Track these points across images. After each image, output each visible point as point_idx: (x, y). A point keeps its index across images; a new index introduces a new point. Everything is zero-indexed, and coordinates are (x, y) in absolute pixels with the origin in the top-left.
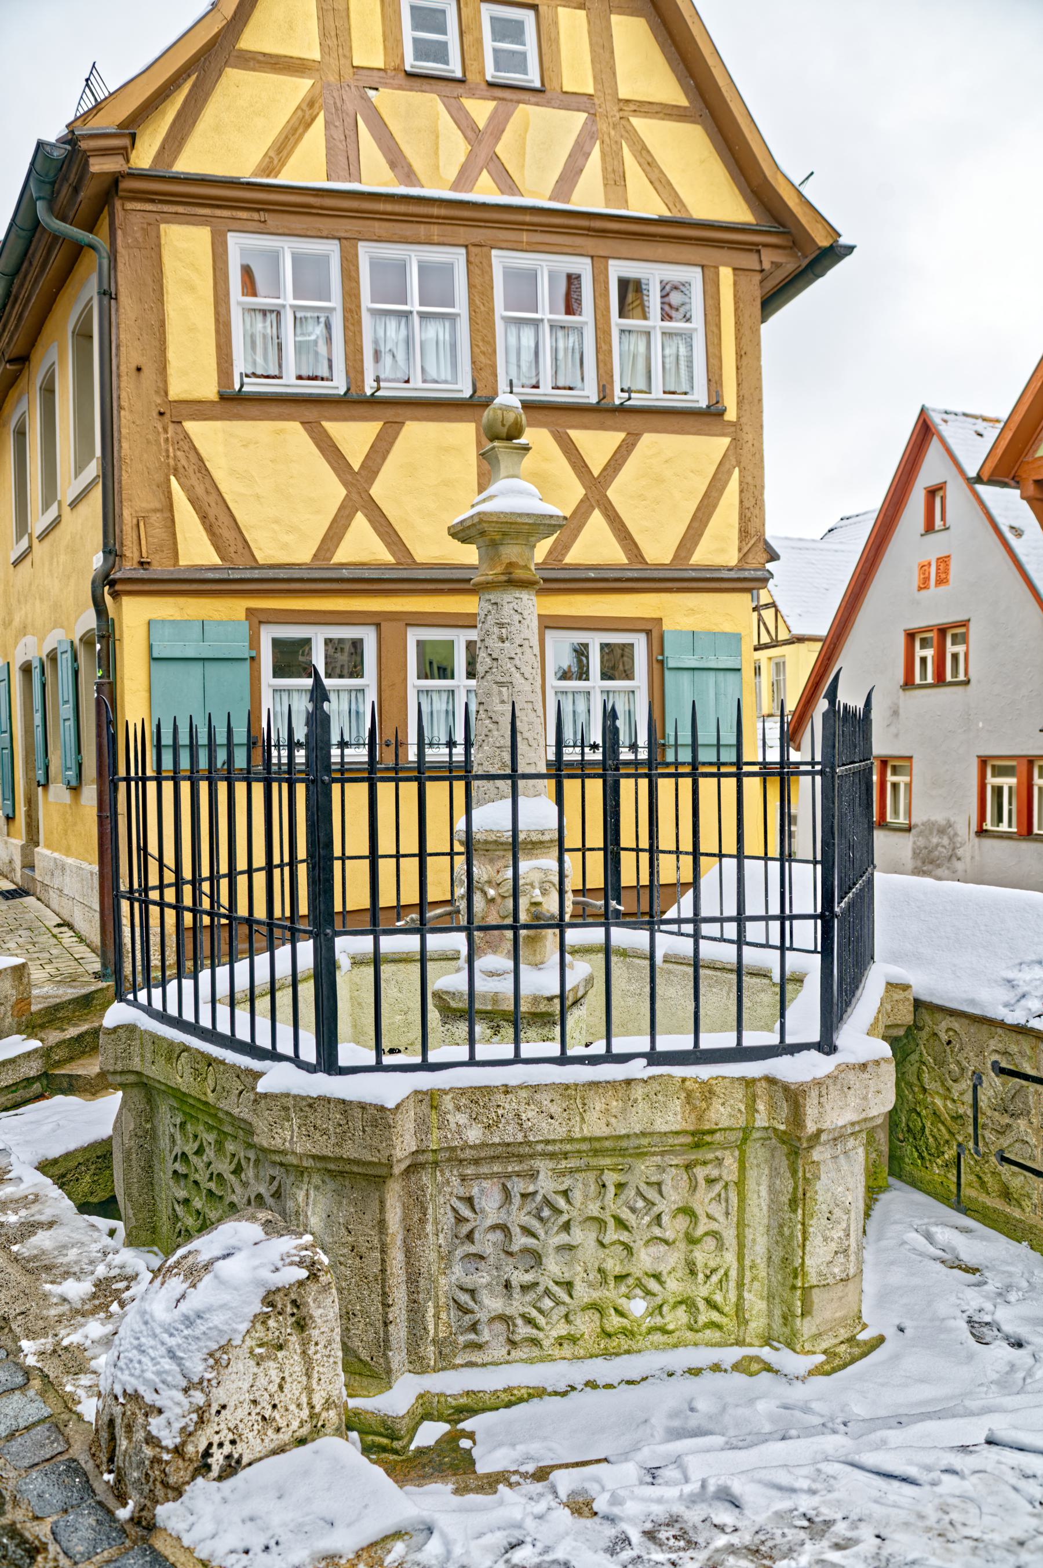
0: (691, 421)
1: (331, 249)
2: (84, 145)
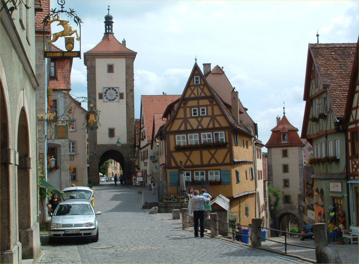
1: (185, 135)
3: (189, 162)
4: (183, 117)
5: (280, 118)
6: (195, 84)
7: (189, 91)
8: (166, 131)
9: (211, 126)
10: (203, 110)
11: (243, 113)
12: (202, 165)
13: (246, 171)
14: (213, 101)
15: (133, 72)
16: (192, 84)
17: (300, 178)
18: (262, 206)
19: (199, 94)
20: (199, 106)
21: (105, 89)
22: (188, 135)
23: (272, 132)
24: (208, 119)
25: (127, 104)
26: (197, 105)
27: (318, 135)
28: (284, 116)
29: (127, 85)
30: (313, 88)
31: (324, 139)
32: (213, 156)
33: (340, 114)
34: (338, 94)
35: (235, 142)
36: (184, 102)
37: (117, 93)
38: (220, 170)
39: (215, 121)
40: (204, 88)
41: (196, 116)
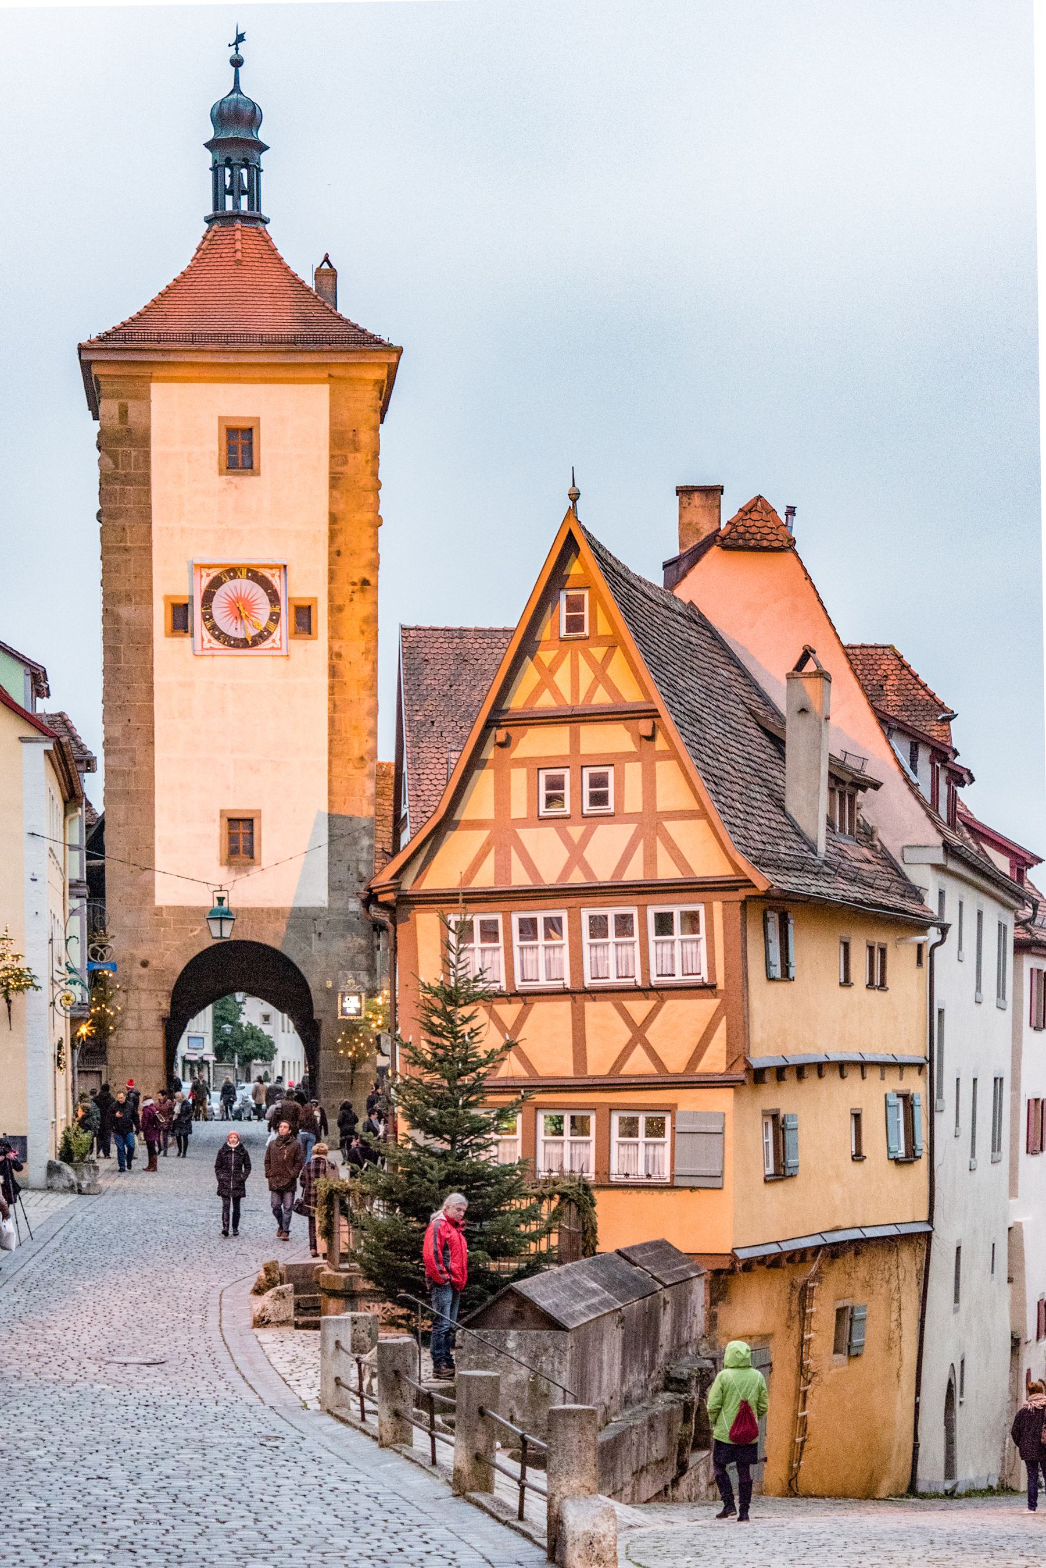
0: (698, 992)
1: (499, 917)
2: (375, 891)
8: (399, 890)
9: (634, 873)
10: (599, 781)
11: (876, 786)
15: (375, 474)
19: (581, 698)
21: (204, 572)
24: (624, 832)
25: (333, 672)
29: (335, 554)
32: (639, 1034)
35: (768, 964)
37: (274, 598)
41: (555, 811)
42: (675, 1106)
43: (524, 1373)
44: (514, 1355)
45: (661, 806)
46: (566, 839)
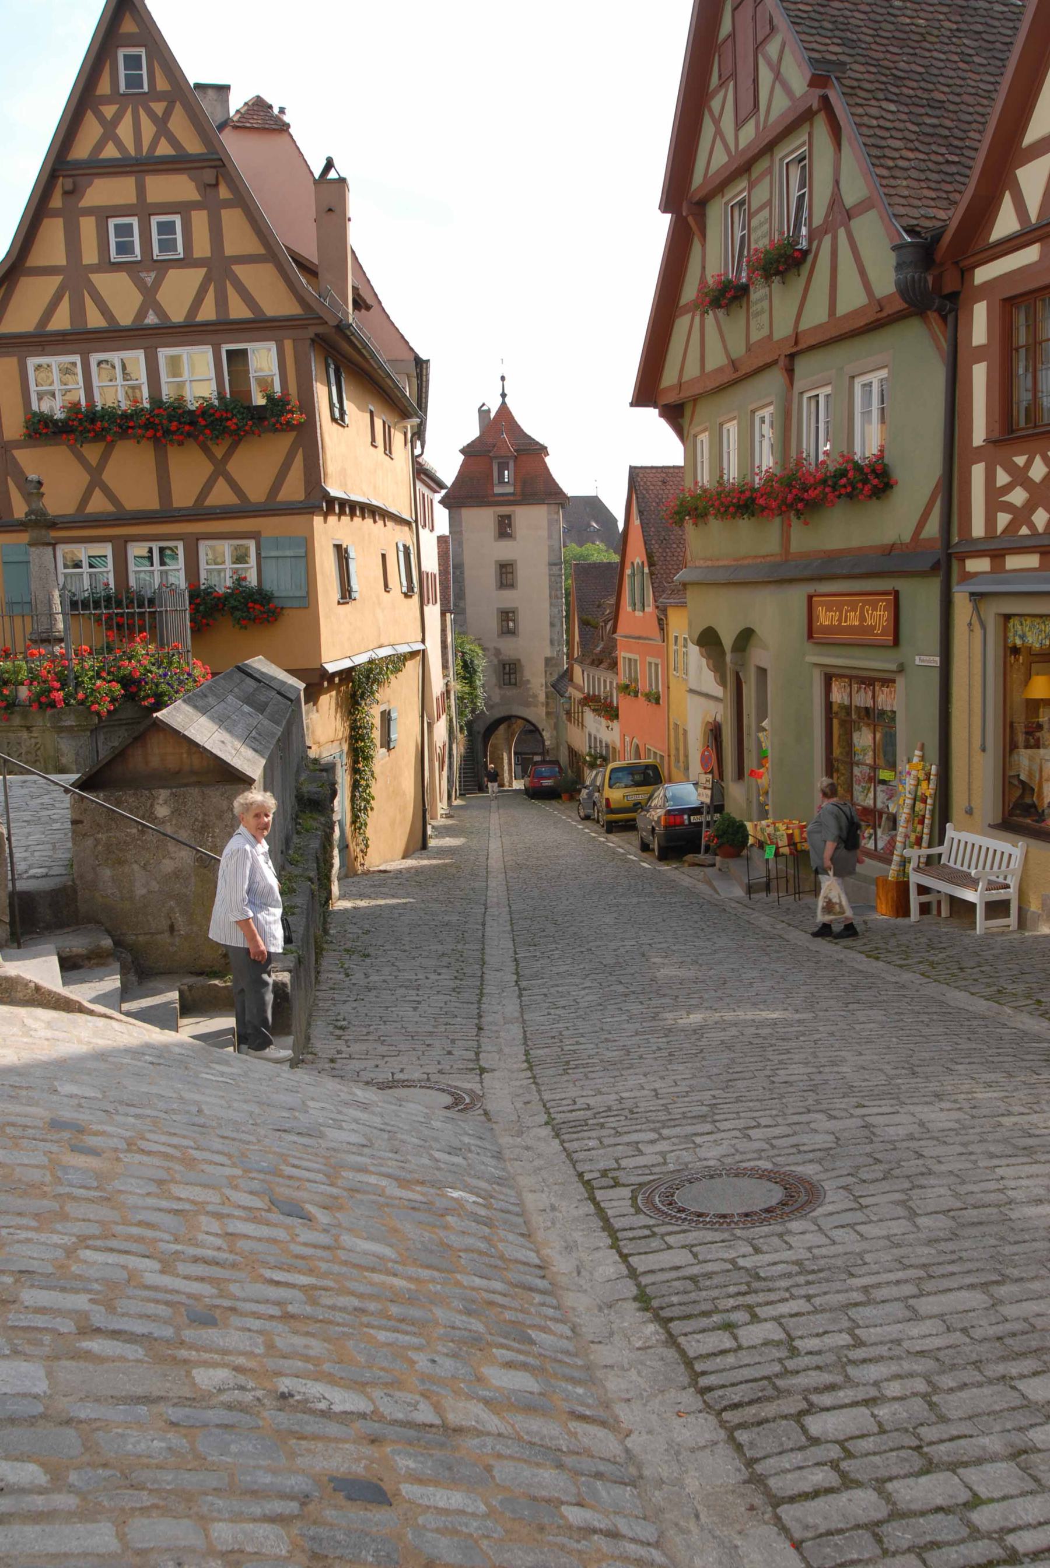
1: (77, 359)
3: (97, 494)
4: (64, 262)
5: (489, 411)
6: (122, 88)
7: (91, 130)
9: (207, 312)
10: (167, 228)
11: (368, 308)
12: (167, 515)
13: (384, 556)
14: (217, 178)
16: (104, 87)
17: (551, 604)
18: (437, 699)
20: (144, 210)
22: (94, 358)
23: (462, 457)
26: (134, 201)
27: (736, 370)
28: (504, 403)
30: (719, 133)
31: (775, 378)
33: (915, 213)
34: (890, 116)
36: (69, 184)
38: (255, 536)
39: (230, 290)
40: (168, 113)
42: (259, 533)
43: (184, 856)
44: (169, 829)
45: (229, 250)
46: (140, 284)
